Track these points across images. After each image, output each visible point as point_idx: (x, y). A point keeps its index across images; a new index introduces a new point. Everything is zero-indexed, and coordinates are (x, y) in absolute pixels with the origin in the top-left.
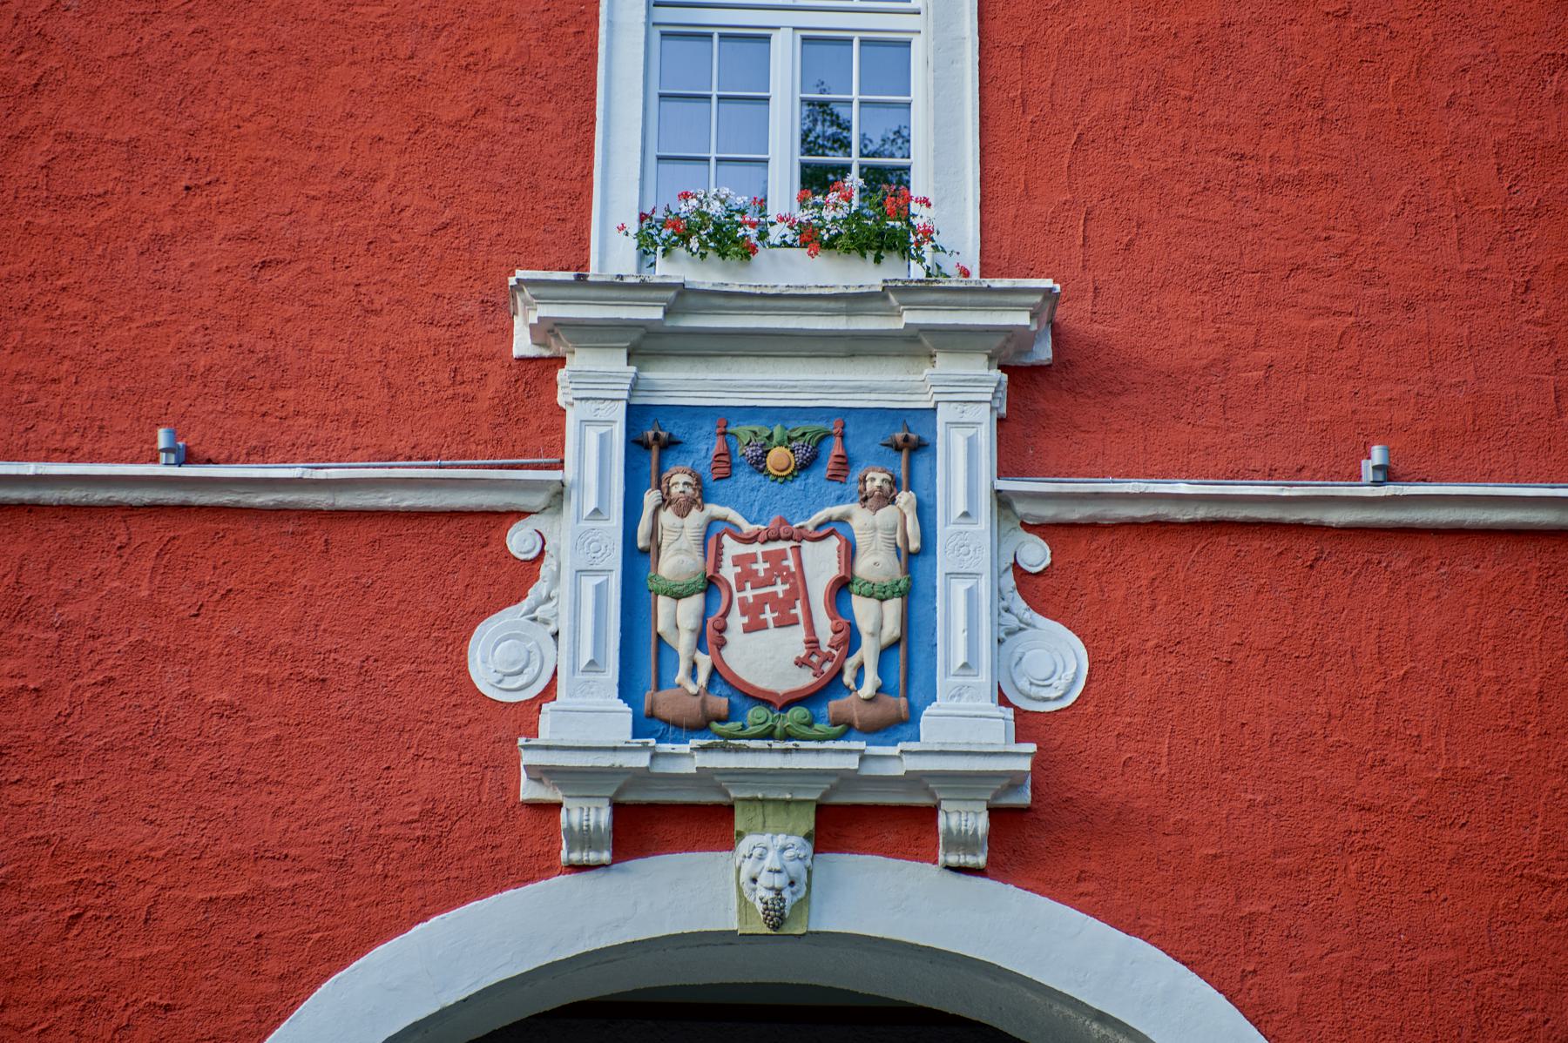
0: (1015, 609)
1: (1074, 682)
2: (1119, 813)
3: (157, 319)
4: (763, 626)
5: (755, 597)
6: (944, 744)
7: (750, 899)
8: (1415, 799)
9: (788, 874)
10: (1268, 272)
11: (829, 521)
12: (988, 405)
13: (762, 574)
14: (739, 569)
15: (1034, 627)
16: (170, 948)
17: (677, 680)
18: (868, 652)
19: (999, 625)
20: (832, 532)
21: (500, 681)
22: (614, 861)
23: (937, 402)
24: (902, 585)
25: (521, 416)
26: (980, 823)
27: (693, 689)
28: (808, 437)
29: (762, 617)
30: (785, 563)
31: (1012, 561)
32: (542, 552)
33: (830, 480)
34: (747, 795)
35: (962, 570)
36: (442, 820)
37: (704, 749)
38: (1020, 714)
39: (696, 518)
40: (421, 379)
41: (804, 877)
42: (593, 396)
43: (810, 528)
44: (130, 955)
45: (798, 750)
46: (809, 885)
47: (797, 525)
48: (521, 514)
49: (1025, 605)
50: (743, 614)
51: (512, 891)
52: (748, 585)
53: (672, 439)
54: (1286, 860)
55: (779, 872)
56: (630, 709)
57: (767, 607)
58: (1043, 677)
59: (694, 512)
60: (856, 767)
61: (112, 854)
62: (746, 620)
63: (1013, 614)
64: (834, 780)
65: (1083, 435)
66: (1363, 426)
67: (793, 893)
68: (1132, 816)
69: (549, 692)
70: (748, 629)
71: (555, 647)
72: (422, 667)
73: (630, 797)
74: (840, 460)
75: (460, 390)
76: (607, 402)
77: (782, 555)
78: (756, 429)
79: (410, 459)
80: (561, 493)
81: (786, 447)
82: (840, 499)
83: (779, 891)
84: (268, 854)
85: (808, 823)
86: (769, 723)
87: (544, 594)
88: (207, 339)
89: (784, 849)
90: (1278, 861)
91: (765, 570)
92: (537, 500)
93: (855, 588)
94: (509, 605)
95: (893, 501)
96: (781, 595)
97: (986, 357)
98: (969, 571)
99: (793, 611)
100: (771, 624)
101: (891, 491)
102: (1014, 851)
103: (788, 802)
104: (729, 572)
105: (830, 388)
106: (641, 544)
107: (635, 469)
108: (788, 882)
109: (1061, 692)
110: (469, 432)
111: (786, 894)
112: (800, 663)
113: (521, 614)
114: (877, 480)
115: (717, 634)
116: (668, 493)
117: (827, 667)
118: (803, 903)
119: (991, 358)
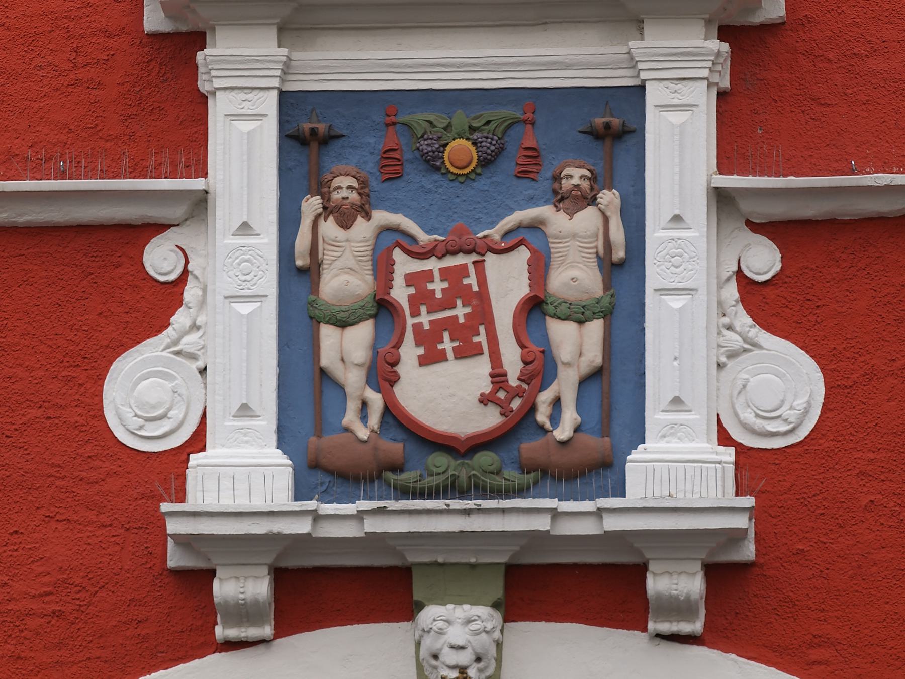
0: (738, 326)
1: (806, 412)
2: (859, 567)
4: (441, 357)
5: (431, 322)
9: (473, 650)
11: (519, 227)
12: (706, 82)
13: (439, 295)
14: (412, 290)
15: (760, 347)
17: (346, 421)
20: (521, 243)
21: (141, 427)
23: (644, 81)
24: (606, 302)
25: (156, 105)
27: (363, 433)
28: (492, 126)
29: (440, 346)
30: (466, 281)
31: (735, 268)
32: (185, 272)
33: (519, 177)
35: (673, 285)
36: (80, 592)
38: (742, 451)
39: (363, 229)
41: (493, 651)
43: (497, 237)
46: (499, 660)
47: (480, 235)
48: (159, 228)
49: (749, 321)
50: (418, 344)
52: (423, 309)
53: (333, 133)
55: (462, 648)
56: (290, 462)
57: (446, 336)
58: (769, 409)
59: (360, 220)
60: (548, 528)
62: (421, 351)
63: (736, 332)
67: (480, 671)
68: (874, 569)
70: (424, 361)
72: (51, 413)
73: (292, 562)
76: (255, 92)
77: (462, 270)
78: (432, 118)
80: (205, 201)
81: (468, 139)
82: (532, 201)
85: (498, 592)
86: (451, 472)
87: (188, 323)
89: (469, 621)
91: (443, 290)
92: (176, 212)
93: (550, 309)
96: (461, 320)
97: (703, 21)
98: (680, 285)
99: (476, 339)
100: (450, 354)
101: (592, 189)
103: (473, 566)
104: (400, 293)
105: (519, 66)
106: (299, 263)
108: (473, 658)
109: (792, 426)
110: (96, 125)
113: (162, 347)
115: (389, 368)
116: (329, 200)
117: (516, 404)
119: (708, 22)
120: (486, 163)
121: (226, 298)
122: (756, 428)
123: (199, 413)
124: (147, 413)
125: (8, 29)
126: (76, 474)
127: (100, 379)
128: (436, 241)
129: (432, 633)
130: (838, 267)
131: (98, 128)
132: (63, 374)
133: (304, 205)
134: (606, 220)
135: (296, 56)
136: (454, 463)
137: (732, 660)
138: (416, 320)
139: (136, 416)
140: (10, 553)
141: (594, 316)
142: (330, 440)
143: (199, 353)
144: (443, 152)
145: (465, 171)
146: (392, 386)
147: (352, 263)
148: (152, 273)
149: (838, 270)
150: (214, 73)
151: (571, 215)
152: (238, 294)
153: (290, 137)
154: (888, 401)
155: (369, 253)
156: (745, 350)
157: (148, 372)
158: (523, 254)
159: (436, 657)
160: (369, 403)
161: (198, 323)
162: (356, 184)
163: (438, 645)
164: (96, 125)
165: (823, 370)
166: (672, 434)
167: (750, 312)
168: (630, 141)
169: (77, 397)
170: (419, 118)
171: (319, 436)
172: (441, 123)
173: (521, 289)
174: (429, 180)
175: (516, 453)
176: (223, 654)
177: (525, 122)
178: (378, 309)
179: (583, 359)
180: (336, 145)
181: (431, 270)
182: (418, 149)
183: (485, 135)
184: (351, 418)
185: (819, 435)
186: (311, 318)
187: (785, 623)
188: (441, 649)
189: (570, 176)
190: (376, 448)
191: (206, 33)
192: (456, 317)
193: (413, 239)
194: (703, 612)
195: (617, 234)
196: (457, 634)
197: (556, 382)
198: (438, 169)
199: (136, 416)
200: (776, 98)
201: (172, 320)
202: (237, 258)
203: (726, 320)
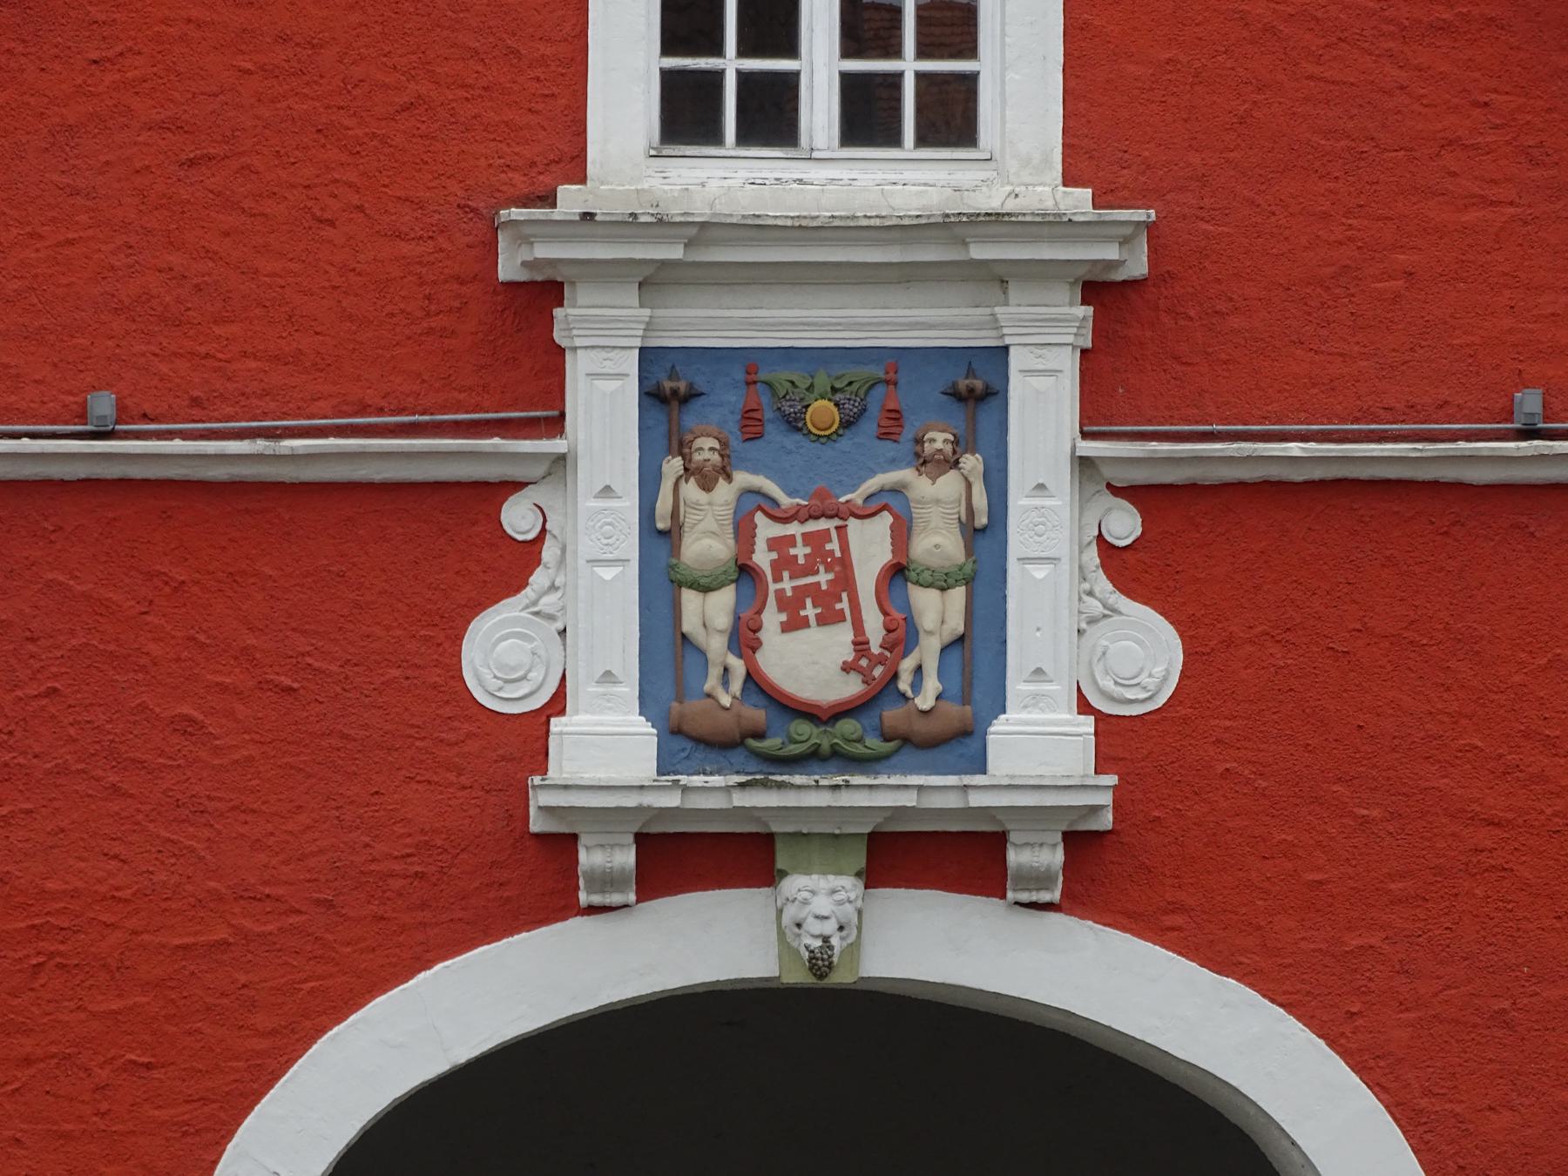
0: (1097, 590)
1: (1165, 679)
2: (1214, 834)
3: (71, 236)
4: (804, 624)
6: (1012, 777)
7: (795, 944)
8: (1549, 811)
9: (836, 917)
10: (1412, 150)
14: (774, 555)
15: (1120, 613)
16: (145, 1000)
18: (928, 651)
19: (1080, 612)
20: (885, 507)
21: (500, 689)
22: (638, 901)
24: (968, 569)
26: (1055, 858)
27: (726, 700)
28: (855, 387)
29: (802, 613)
30: (828, 547)
31: (1096, 533)
32: (543, 531)
34: (790, 829)
35: (1036, 554)
36: (441, 853)
37: (742, 786)
38: (1100, 717)
39: (725, 492)
40: (389, 309)
42: (601, 344)
43: (860, 502)
44: (104, 1007)
45: (848, 786)
46: (859, 928)
47: (842, 499)
48: (517, 486)
49: (1110, 587)
50: (781, 609)
51: (524, 934)
52: (786, 574)
53: (693, 392)
54: (1400, 885)
55: (826, 918)
56: (655, 731)
57: (809, 602)
59: (722, 482)
61: (75, 894)
62: (783, 617)
63: (1096, 598)
64: (888, 814)
65: (1184, 368)
66: (1520, 349)
67: (842, 939)
68: (1229, 837)
69: (557, 704)
70: (787, 628)
71: (562, 647)
72: (409, 673)
74: (893, 415)
75: (435, 322)
77: (825, 536)
78: (794, 378)
79: (380, 411)
81: (830, 400)
82: (894, 464)
83: (826, 939)
84: (246, 894)
85: (861, 862)
87: (547, 584)
88: (130, 260)
89: (834, 892)
90: (1392, 886)
92: (537, 471)
93: (913, 575)
94: (508, 596)
95: (956, 464)
99: (838, 606)
100: (812, 621)
101: (954, 452)
102: (1093, 880)
104: (762, 558)
105: (880, 325)
106: (660, 525)
107: (649, 428)
108: (837, 927)
109: (1150, 693)
110: (450, 375)
111: (835, 941)
113: (520, 608)
114: (939, 441)
116: (690, 461)
117: (878, 671)
118: (854, 949)
119: (1073, 284)
120: (847, 424)
121: (588, 561)
122: (1115, 695)
123: (560, 675)
124: (507, 674)
125: (359, 274)
126: (436, 735)
127: (458, 639)
128: (798, 505)
129: (797, 902)
130: (1199, 532)
131: (452, 379)
132: (422, 633)
133: (665, 467)
134: (969, 486)
135: (659, 312)
136: (816, 731)
137: (1089, 926)
138: (779, 586)
139: (495, 677)
140: (371, 814)
141: (957, 583)
142: (694, 705)
143: (559, 614)
144: (805, 413)
145: (827, 433)
146: (754, 653)
147: (714, 527)
148: (510, 531)
149: (1198, 535)
150: (575, 332)
152: (600, 558)
153: (648, 394)
154: (1246, 668)
155: (731, 516)
156: (1105, 616)
157: (507, 634)
158: (886, 519)
159: (799, 925)
160: (731, 670)
161: (557, 583)
162: (717, 446)
163: (802, 915)
164: (450, 375)
165: (1181, 636)
166: (1034, 705)
167: (1111, 578)
168: (994, 403)
169: (435, 657)
170: (781, 376)
171: (681, 702)
172: (803, 384)
175: (877, 720)
176: (586, 917)
177: (887, 382)
178: (740, 574)
179: (945, 627)
180: (696, 405)
181: (794, 536)
182: (779, 409)
183: (848, 396)
184: (712, 683)
185: (1177, 703)
186: (672, 581)
188: (805, 919)
189: (933, 440)
190: (739, 716)
192: (818, 584)
194: (1061, 879)
195: (980, 500)
196: (822, 905)
197: (917, 649)
198: (799, 430)
199: (495, 677)
200: (1138, 356)
201: (531, 579)
202: (599, 521)
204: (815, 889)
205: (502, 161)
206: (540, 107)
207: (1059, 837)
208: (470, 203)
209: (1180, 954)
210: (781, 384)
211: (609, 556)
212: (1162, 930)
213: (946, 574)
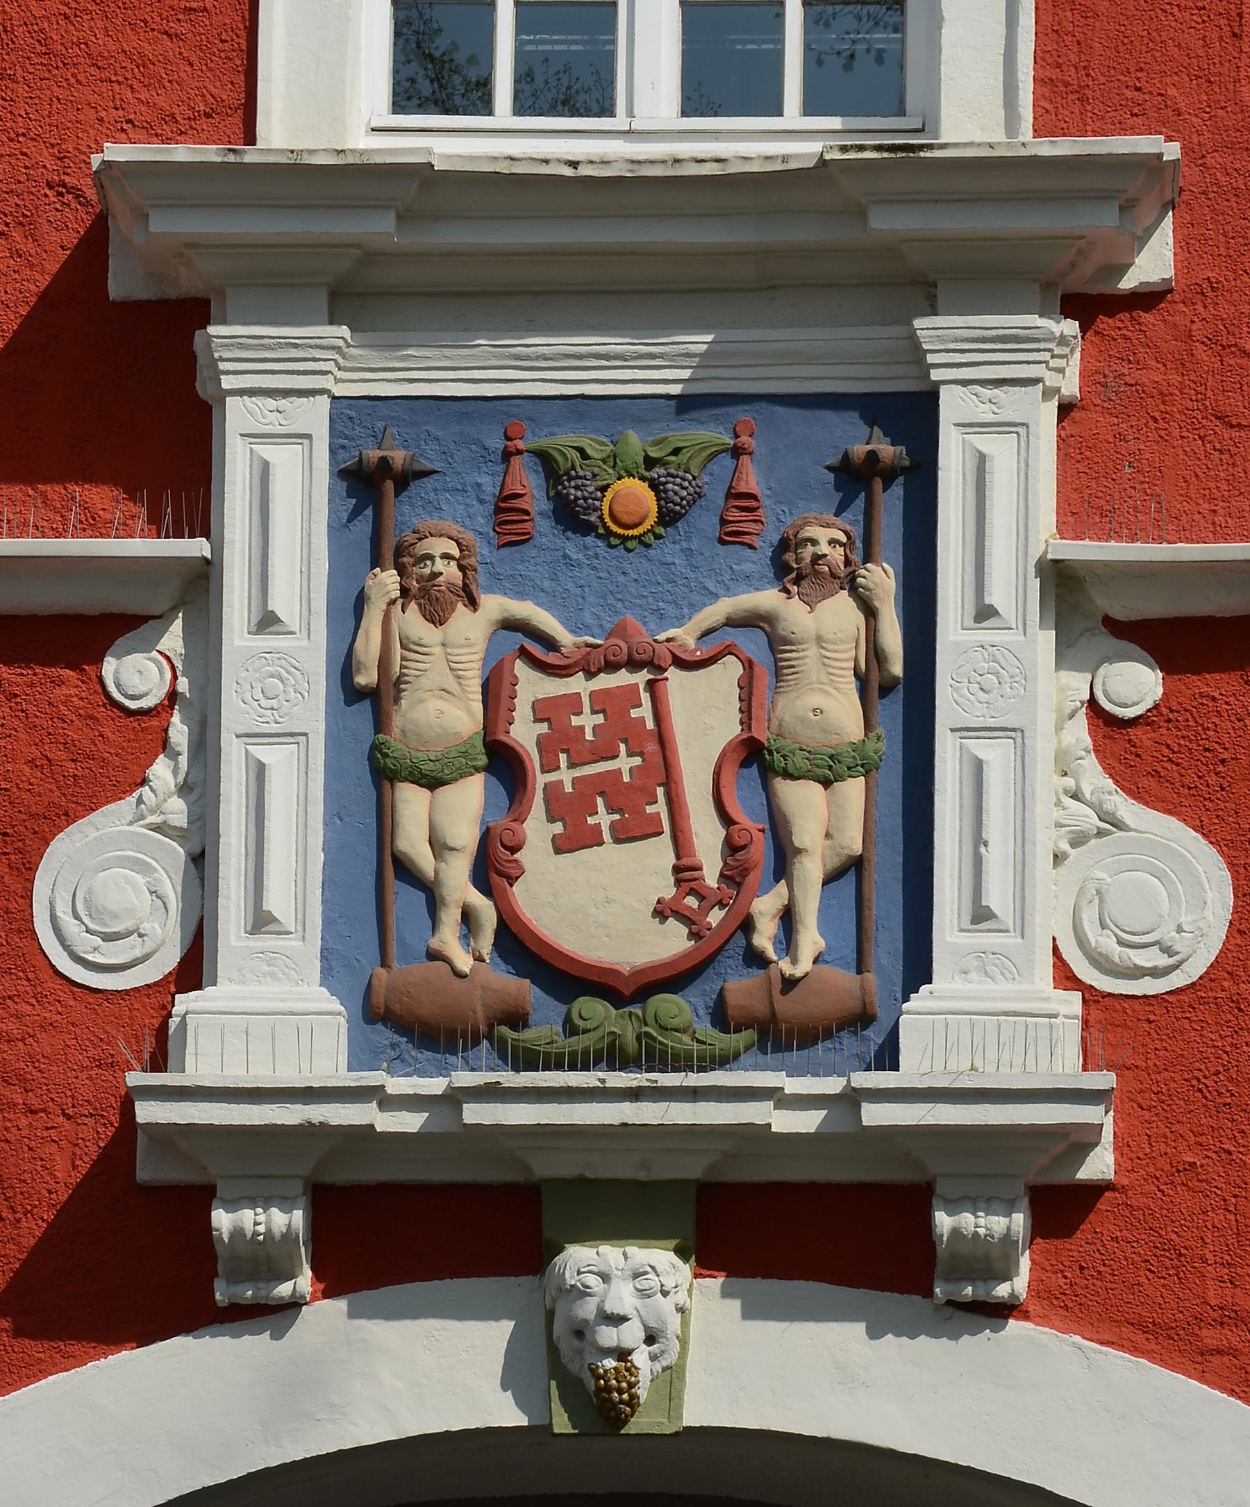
7: (574, 1368)
20: (729, 650)
23: (938, 384)
27: (464, 962)
28: (683, 457)
38: (1091, 997)
43: (691, 642)
46: (684, 1341)
47: (662, 637)
53: (417, 467)
65: (1235, 433)
67: (653, 1358)
77: (629, 696)
78: (584, 442)
81: (642, 478)
82: (750, 582)
97: (1037, 285)
100: (606, 835)
101: (848, 562)
106: (361, 680)
108: (642, 1335)
111: (640, 1358)
112: (662, 912)
117: (715, 917)
118: (672, 1377)
120: (668, 518)
128: (588, 645)
134: (870, 612)
137: (1074, 1345)
141: (851, 771)
145: (635, 532)
146: (511, 886)
151: (811, 606)
152: (257, 730)
156: (1100, 833)
158: (730, 669)
162: (456, 552)
165: (1231, 865)
173: (729, 729)
174: (573, 546)
187: (1164, 1286)
191: (209, 301)
192: (618, 772)
193: (550, 644)
200: (1156, 414)
203: (1070, 782)
204: (603, 1268)
205: (121, 113)
206: (184, 28)
207: (1021, 1189)
208: (67, 179)
209: (1232, 1393)
210: (564, 454)
211: (274, 728)
212: (1202, 1354)
213: (832, 757)
